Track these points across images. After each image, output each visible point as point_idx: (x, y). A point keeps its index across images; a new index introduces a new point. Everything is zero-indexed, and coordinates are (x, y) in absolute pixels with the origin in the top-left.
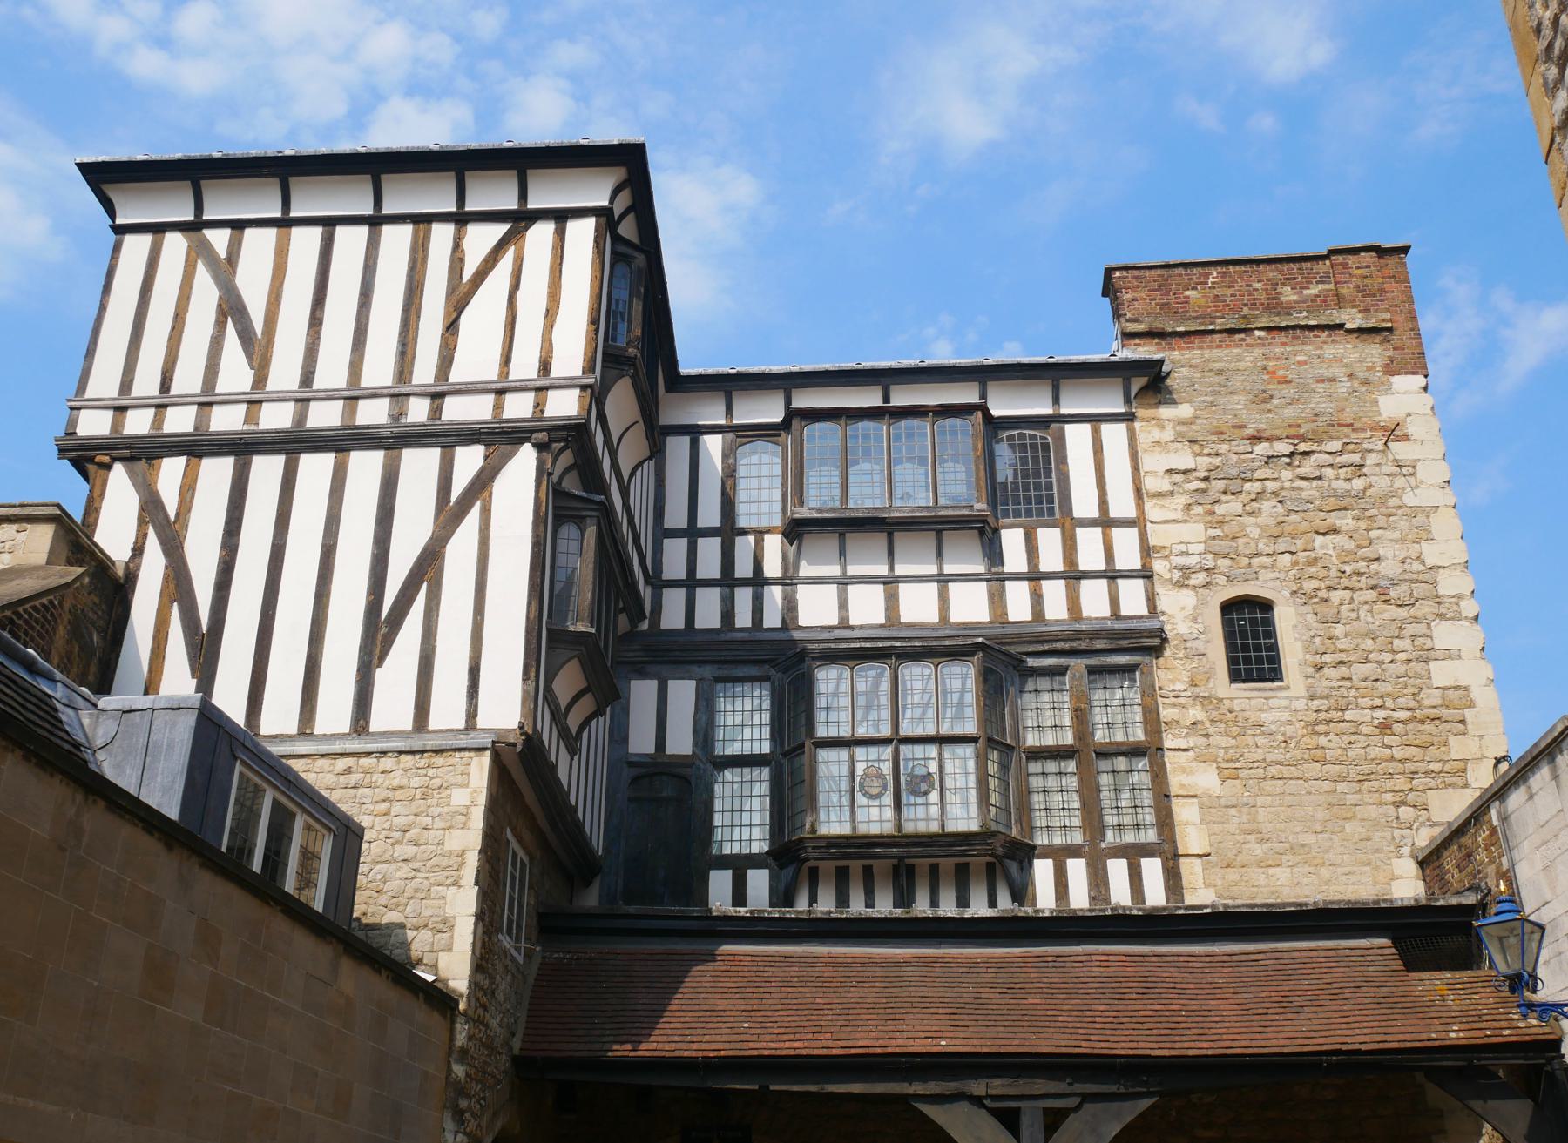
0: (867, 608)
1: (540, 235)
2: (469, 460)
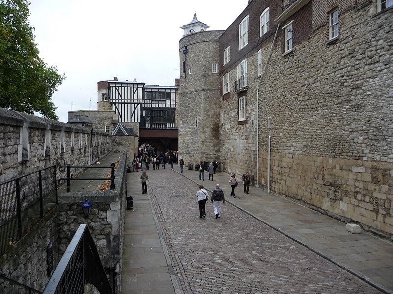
0: (157, 106)
1: (139, 89)
2: (136, 105)
